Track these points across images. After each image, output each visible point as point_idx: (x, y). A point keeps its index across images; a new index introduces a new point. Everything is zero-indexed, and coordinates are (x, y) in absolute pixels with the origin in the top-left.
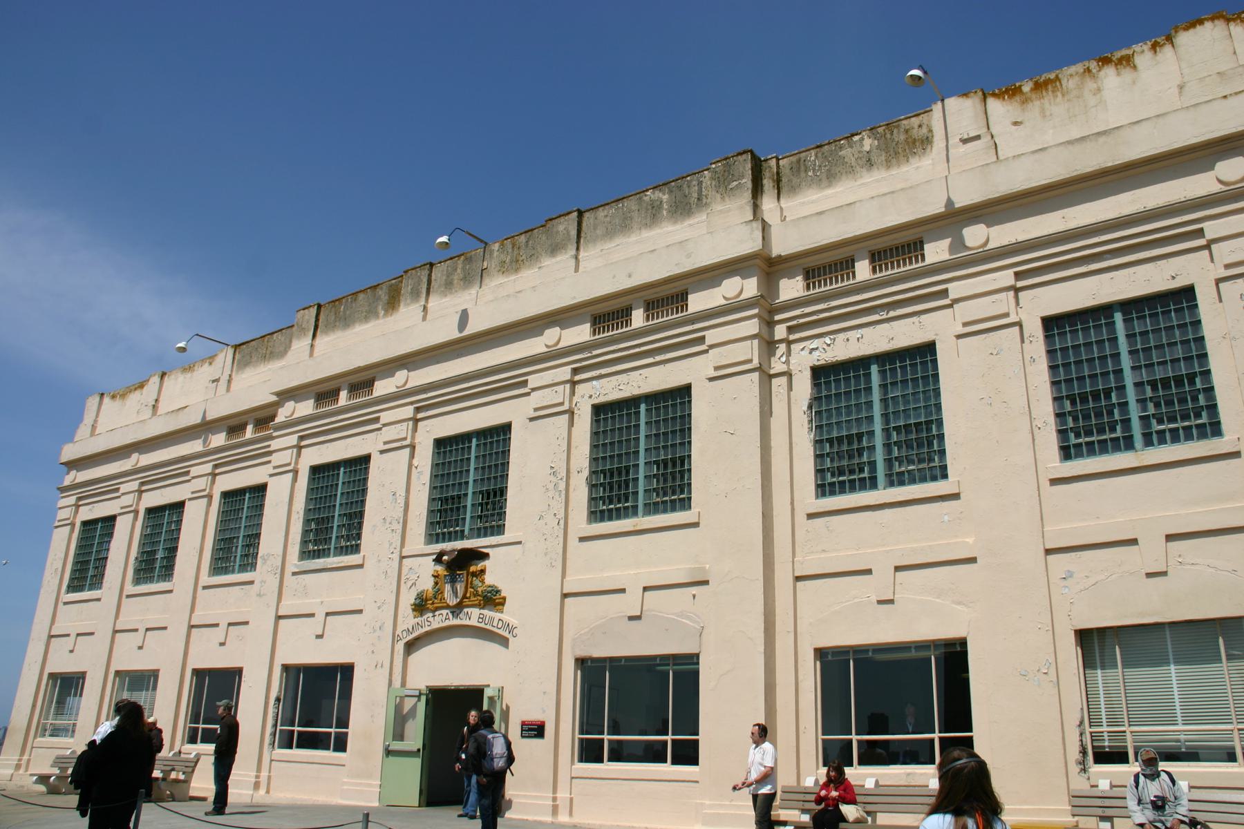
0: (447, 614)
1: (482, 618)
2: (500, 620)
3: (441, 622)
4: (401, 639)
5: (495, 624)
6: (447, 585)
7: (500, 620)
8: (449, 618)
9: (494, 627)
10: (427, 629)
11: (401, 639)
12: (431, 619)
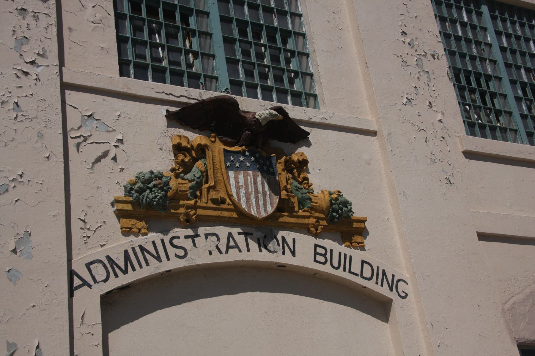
0: (230, 235)
1: (324, 255)
2: (363, 262)
3: (215, 252)
4: (85, 283)
5: (356, 268)
6: (231, 173)
7: (363, 262)
8: (237, 246)
9: (357, 275)
10: (175, 264)
11: (85, 283)
12: (188, 244)
